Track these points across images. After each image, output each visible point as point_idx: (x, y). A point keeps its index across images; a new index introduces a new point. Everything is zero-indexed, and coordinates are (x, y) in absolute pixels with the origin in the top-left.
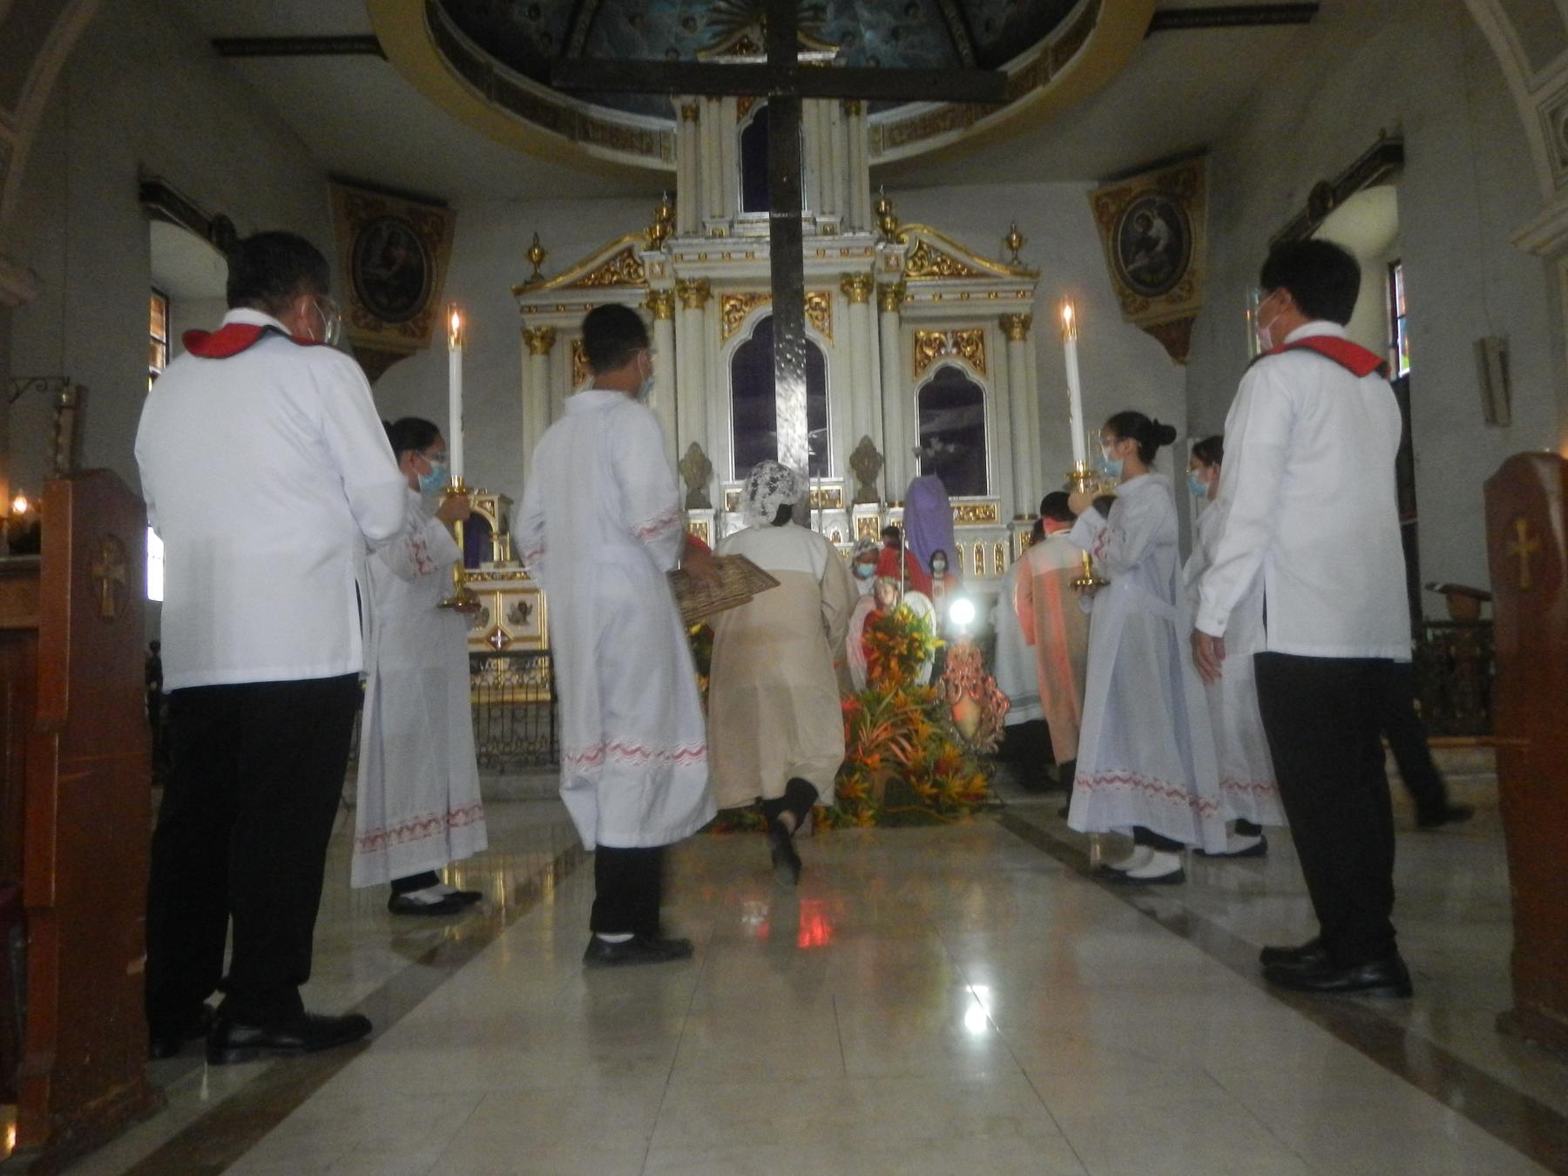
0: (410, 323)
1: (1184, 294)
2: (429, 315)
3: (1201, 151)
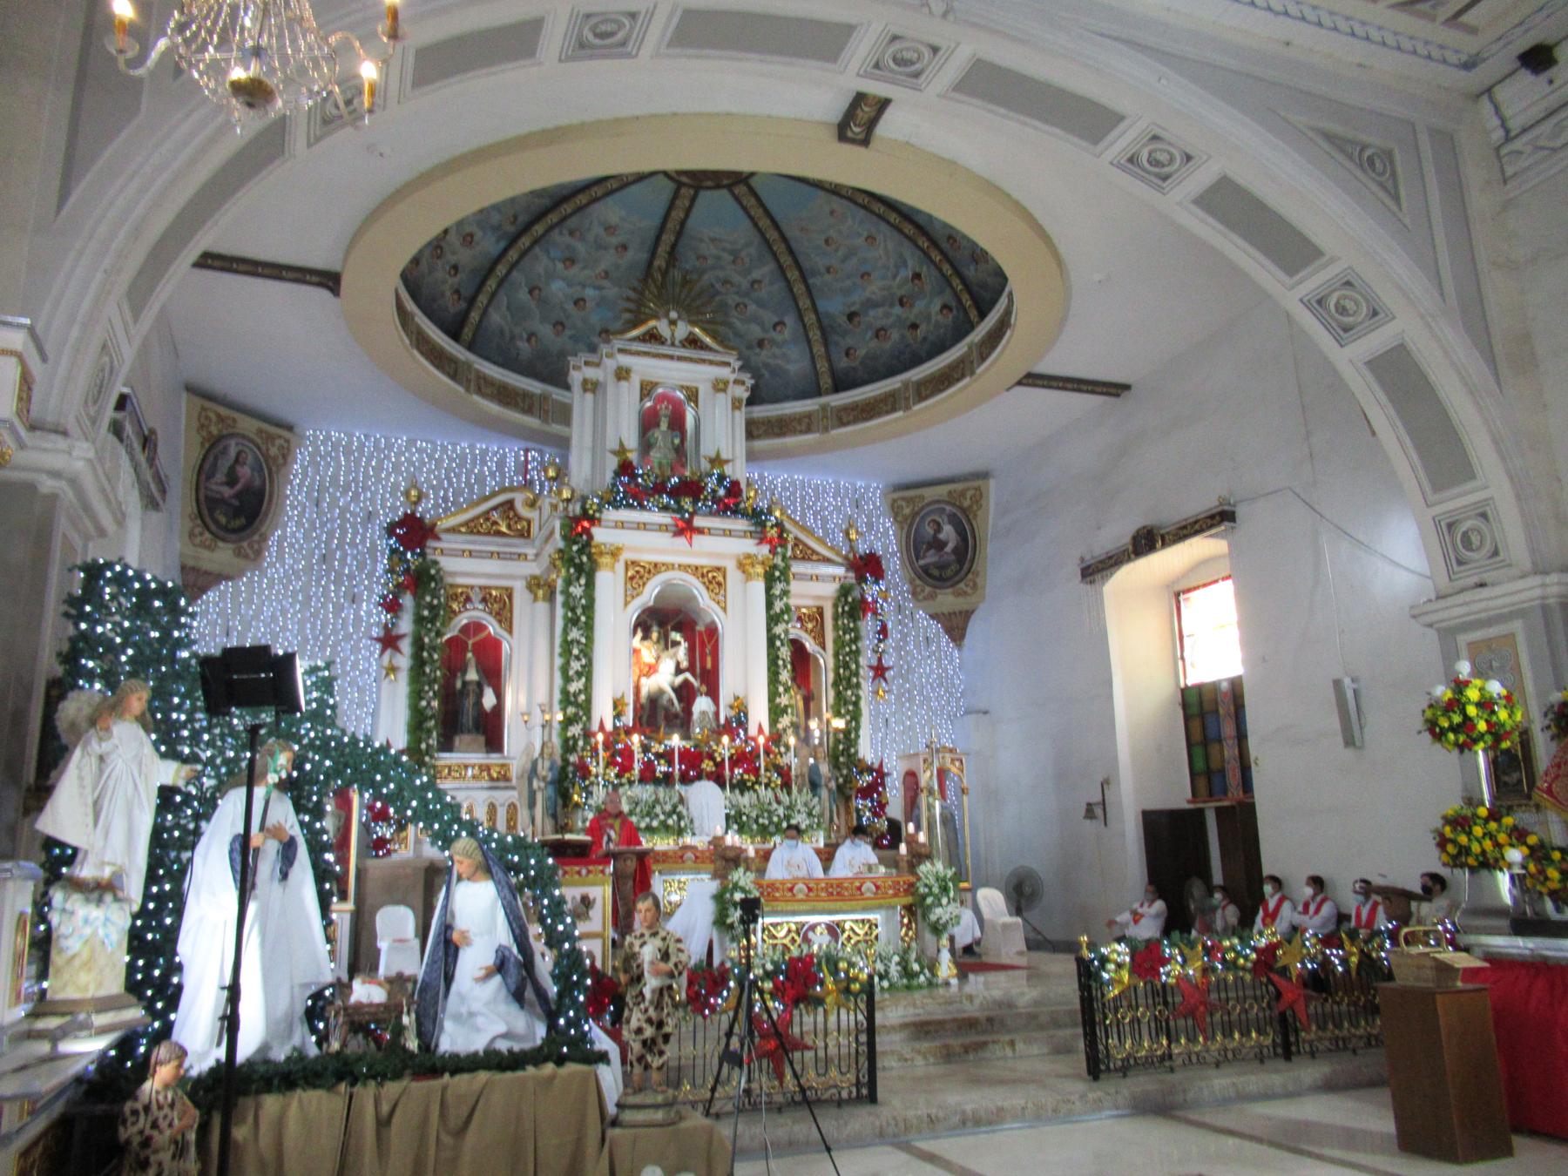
0: (245, 544)
1: (969, 590)
2: (264, 538)
3: (984, 475)
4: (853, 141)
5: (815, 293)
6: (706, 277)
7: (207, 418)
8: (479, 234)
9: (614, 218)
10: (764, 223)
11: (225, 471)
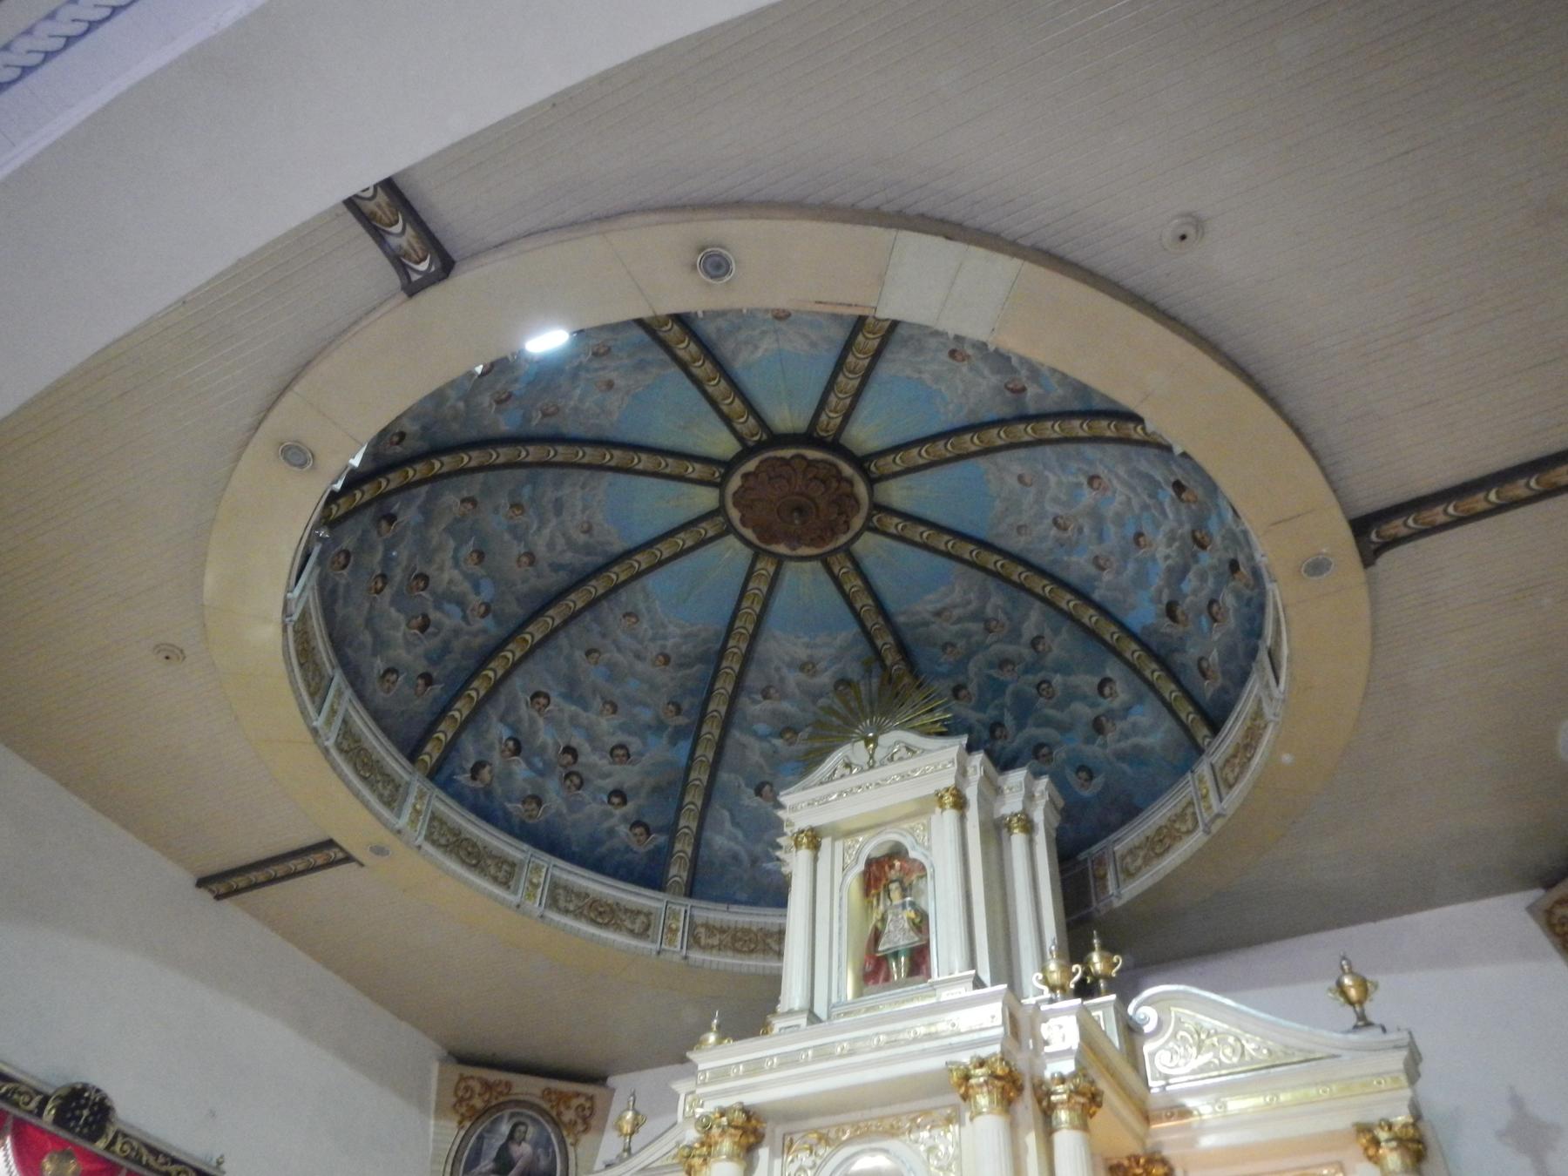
4: (430, 281)
5: (1112, 610)
6: (972, 668)
7: (467, 1088)
8: (635, 744)
9: (802, 654)
10: (967, 550)
11: (493, 1154)
